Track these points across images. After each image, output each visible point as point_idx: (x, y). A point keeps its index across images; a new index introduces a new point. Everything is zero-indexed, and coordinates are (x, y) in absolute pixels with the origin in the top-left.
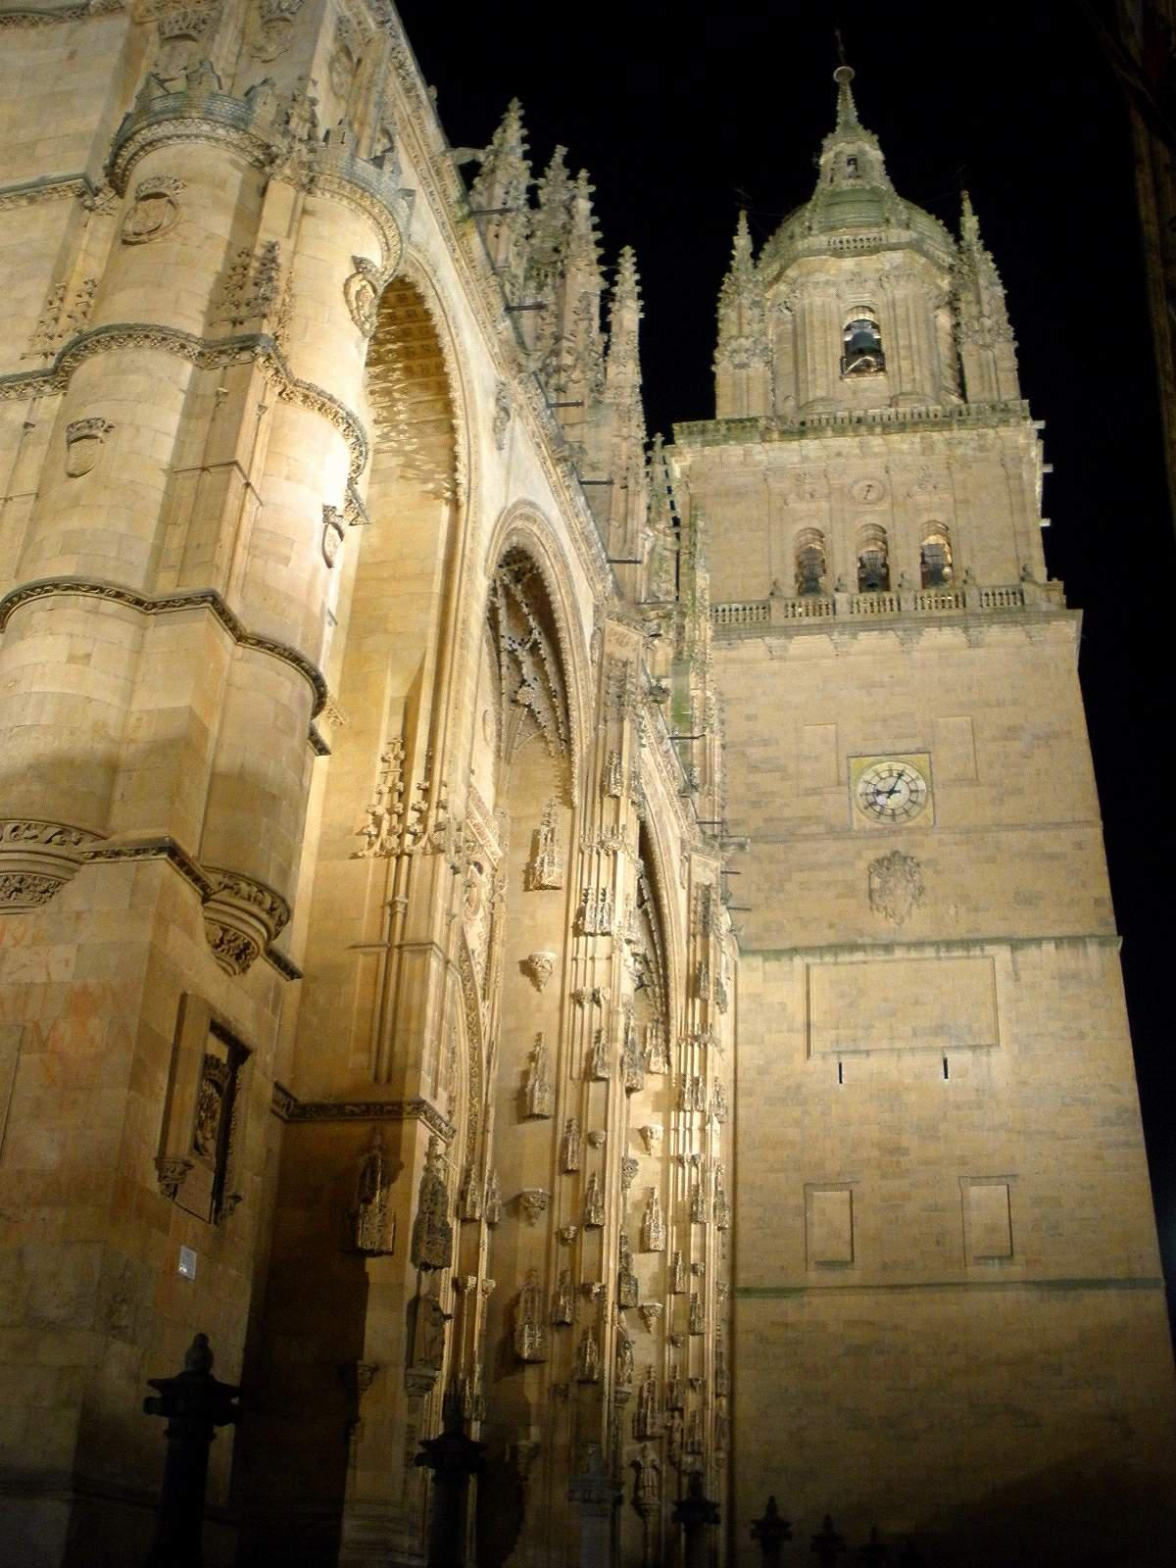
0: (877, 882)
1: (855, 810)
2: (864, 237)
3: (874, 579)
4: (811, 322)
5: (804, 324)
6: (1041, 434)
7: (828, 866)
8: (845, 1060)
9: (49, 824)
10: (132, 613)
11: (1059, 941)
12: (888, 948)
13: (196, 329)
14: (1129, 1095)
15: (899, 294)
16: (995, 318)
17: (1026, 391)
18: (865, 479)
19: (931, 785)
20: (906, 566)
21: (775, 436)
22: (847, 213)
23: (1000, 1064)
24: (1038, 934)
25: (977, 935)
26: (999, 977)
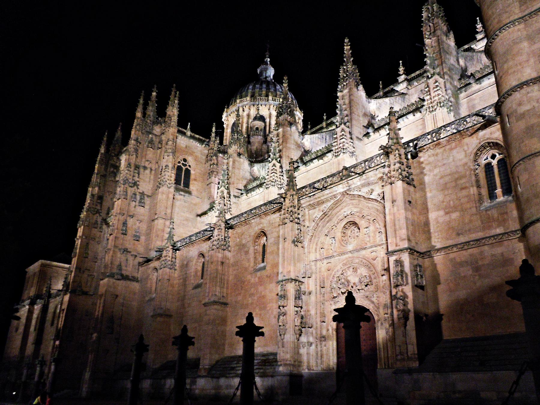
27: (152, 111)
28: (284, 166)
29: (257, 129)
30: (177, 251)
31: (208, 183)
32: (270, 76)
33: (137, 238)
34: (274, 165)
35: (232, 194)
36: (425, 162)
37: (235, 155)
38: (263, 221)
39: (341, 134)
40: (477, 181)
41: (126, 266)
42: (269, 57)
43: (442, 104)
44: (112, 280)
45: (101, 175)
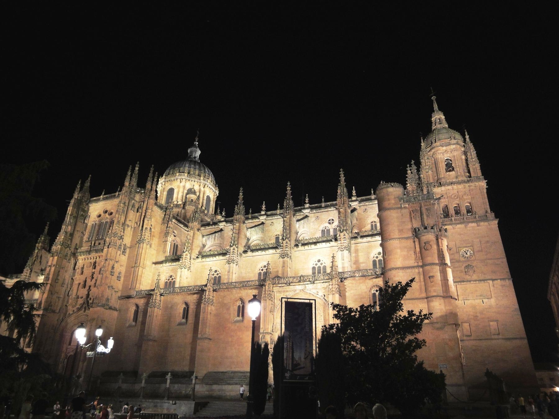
0: (466, 270)
3: (457, 212)
7: (457, 267)
8: (465, 301)
10: (442, 298)
11: (501, 279)
12: (470, 281)
13: (437, 262)
14: (517, 306)
15: (455, 154)
16: (475, 159)
18: (454, 194)
20: (464, 211)
21: (436, 187)
22: (441, 136)
27: (135, 182)
28: (239, 250)
29: (192, 200)
31: (164, 241)
32: (197, 157)
33: (119, 278)
34: (234, 249)
35: (192, 257)
37: (196, 229)
38: (242, 292)
39: (286, 245)
40: (370, 300)
41: (111, 299)
42: (197, 141)
43: (347, 249)
44: (102, 309)
45: (73, 217)
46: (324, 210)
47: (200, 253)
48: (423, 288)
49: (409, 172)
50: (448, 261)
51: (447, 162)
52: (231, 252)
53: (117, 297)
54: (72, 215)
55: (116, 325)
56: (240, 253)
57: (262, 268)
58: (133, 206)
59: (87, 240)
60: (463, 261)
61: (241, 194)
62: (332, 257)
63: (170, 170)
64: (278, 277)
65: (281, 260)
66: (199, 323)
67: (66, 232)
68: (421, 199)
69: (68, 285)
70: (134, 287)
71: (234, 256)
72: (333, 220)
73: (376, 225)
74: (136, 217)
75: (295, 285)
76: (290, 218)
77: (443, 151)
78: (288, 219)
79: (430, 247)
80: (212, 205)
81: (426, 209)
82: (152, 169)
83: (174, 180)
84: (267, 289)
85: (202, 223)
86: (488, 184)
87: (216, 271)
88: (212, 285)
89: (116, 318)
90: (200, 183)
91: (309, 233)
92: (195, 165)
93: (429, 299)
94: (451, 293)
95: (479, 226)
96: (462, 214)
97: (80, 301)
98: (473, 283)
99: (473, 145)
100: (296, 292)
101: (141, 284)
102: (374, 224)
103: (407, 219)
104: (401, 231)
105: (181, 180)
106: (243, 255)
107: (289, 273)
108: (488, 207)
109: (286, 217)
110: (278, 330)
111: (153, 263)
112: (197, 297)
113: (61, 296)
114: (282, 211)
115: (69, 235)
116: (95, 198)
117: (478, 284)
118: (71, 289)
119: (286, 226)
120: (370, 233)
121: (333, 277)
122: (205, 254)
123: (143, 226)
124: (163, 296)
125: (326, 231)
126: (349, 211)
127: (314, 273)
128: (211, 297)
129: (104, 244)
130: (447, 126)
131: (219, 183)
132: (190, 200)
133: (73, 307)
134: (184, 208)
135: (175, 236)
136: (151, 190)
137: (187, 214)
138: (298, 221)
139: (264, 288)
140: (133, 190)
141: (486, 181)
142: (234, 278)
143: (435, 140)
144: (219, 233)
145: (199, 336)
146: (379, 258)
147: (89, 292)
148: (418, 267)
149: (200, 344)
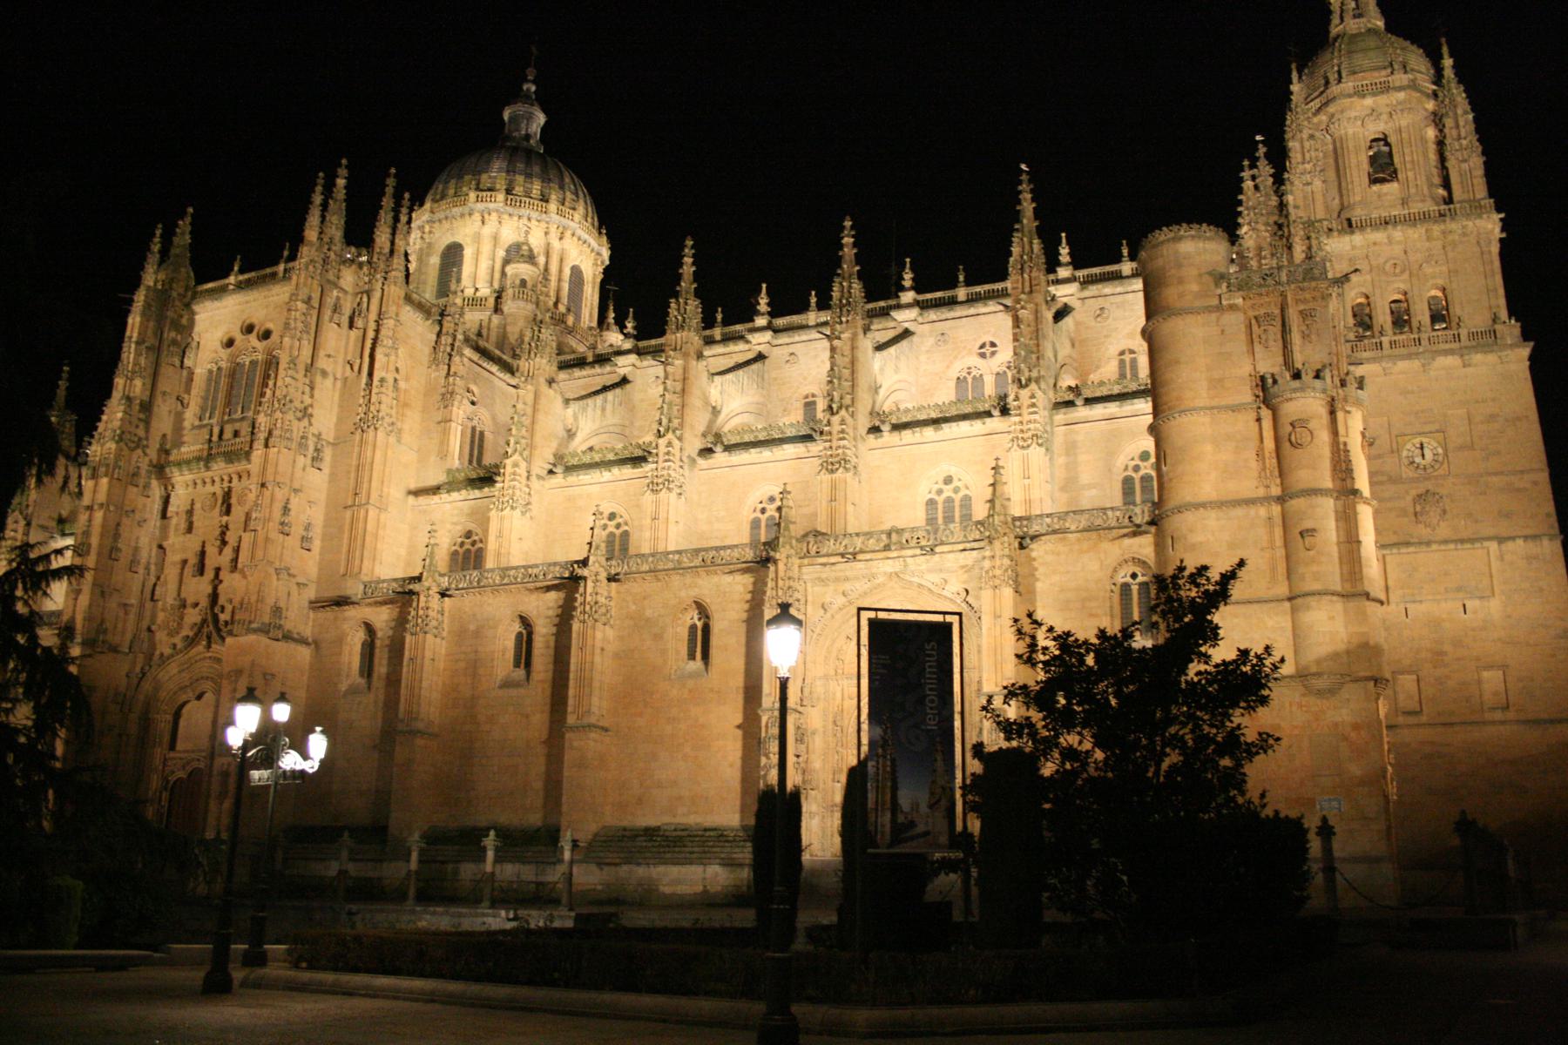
0: (1418, 508)
1: (1403, 467)
2: (1378, 81)
3: (1401, 320)
4: (1348, 147)
5: (1343, 149)
6: (1501, 220)
7: (1390, 499)
8: (1408, 606)
9: (1336, 674)
10: (1340, 599)
11: (1526, 538)
12: (1428, 543)
13: (1328, 483)
15: (1404, 123)
16: (1468, 139)
17: (1492, 193)
18: (1394, 259)
19: (1446, 450)
20: (1421, 314)
22: (1360, 60)
23: (1495, 606)
24: (1514, 534)
25: (1479, 536)
26: (1492, 559)
28: (686, 445)
29: (523, 283)
30: (446, 599)
31: (440, 419)
32: (536, 134)
33: (305, 542)
34: (669, 444)
35: (534, 473)
36: (1040, 560)
37: (542, 380)
38: (700, 582)
40: (1111, 607)
41: (287, 610)
42: (534, 82)
43: (1040, 441)
44: (264, 640)
45: (146, 347)
46: (965, 313)
47: (559, 457)
48: (1281, 568)
49: (1248, 185)
50: (1362, 483)
51: (1375, 149)
52: (661, 454)
53: (307, 604)
54: (144, 342)
55: (308, 687)
56: (689, 457)
57: (761, 506)
58: (336, 309)
59: (197, 423)
60: (1413, 480)
61: (688, 260)
62: (993, 468)
63: (447, 182)
64: (817, 534)
65: (826, 477)
66: (567, 679)
67: (129, 399)
68: (1284, 279)
69: (147, 568)
70: (356, 570)
71: (669, 468)
72: (993, 345)
73: (1134, 362)
74: (347, 343)
75: (871, 560)
76: (854, 339)
77: (1363, 114)
78: (845, 344)
79: (1309, 439)
80: (591, 295)
81: (1301, 312)
82: (391, 182)
83: (462, 215)
84: (781, 574)
85: (562, 358)
86: (1506, 225)
87: (612, 516)
88: (603, 560)
89: (307, 667)
90: (547, 223)
91: (913, 389)
92: (528, 163)
93: (1299, 601)
94: (1366, 583)
95: (1469, 365)
96: (1415, 324)
97: (193, 616)
98: (1436, 551)
99: (1465, 91)
100: (877, 581)
101: (377, 562)
102: (1127, 357)
103: (1240, 344)
104: (1216, 384)
105: (486, 216)
106: (701, 462)
107: (851, 519)
108: (1502, 302)
109: (839, 338)
110: (818, 699)
111: (410, 493)
112: (556, 601)
113: (133, 601)
114: (825, 316)
115: (137, 407)
116: (210, 285)
117: (1455, 553)
118: (158, 578)
119: (838, 366)
120: (1116, 390)
121: (996, 531)
122: (575, 461)
123: (370, 374)
124: (450, 596)
125: (970, 380)
126: (1049, 315)
127: (931, 521)
128: (602, 600)
129: (253, 433)
130: (1380, 24)
131: (609, 221)
132: (518, 282)
133: (171, 634)
134: (497, 309)
135: (473, 403)
136: (392, 252)
137: (509, 329)
138: (880, 347)
139: (772, 568)
140: (332, 255)
141: (1502, 215)
142: (674, 539)
143: (1339, 73)
144: (618, 391)
145: (571, 720)
146: (1142, 472)
147: (215, 588)
148: (1267, 499)
149: (575, 744)
